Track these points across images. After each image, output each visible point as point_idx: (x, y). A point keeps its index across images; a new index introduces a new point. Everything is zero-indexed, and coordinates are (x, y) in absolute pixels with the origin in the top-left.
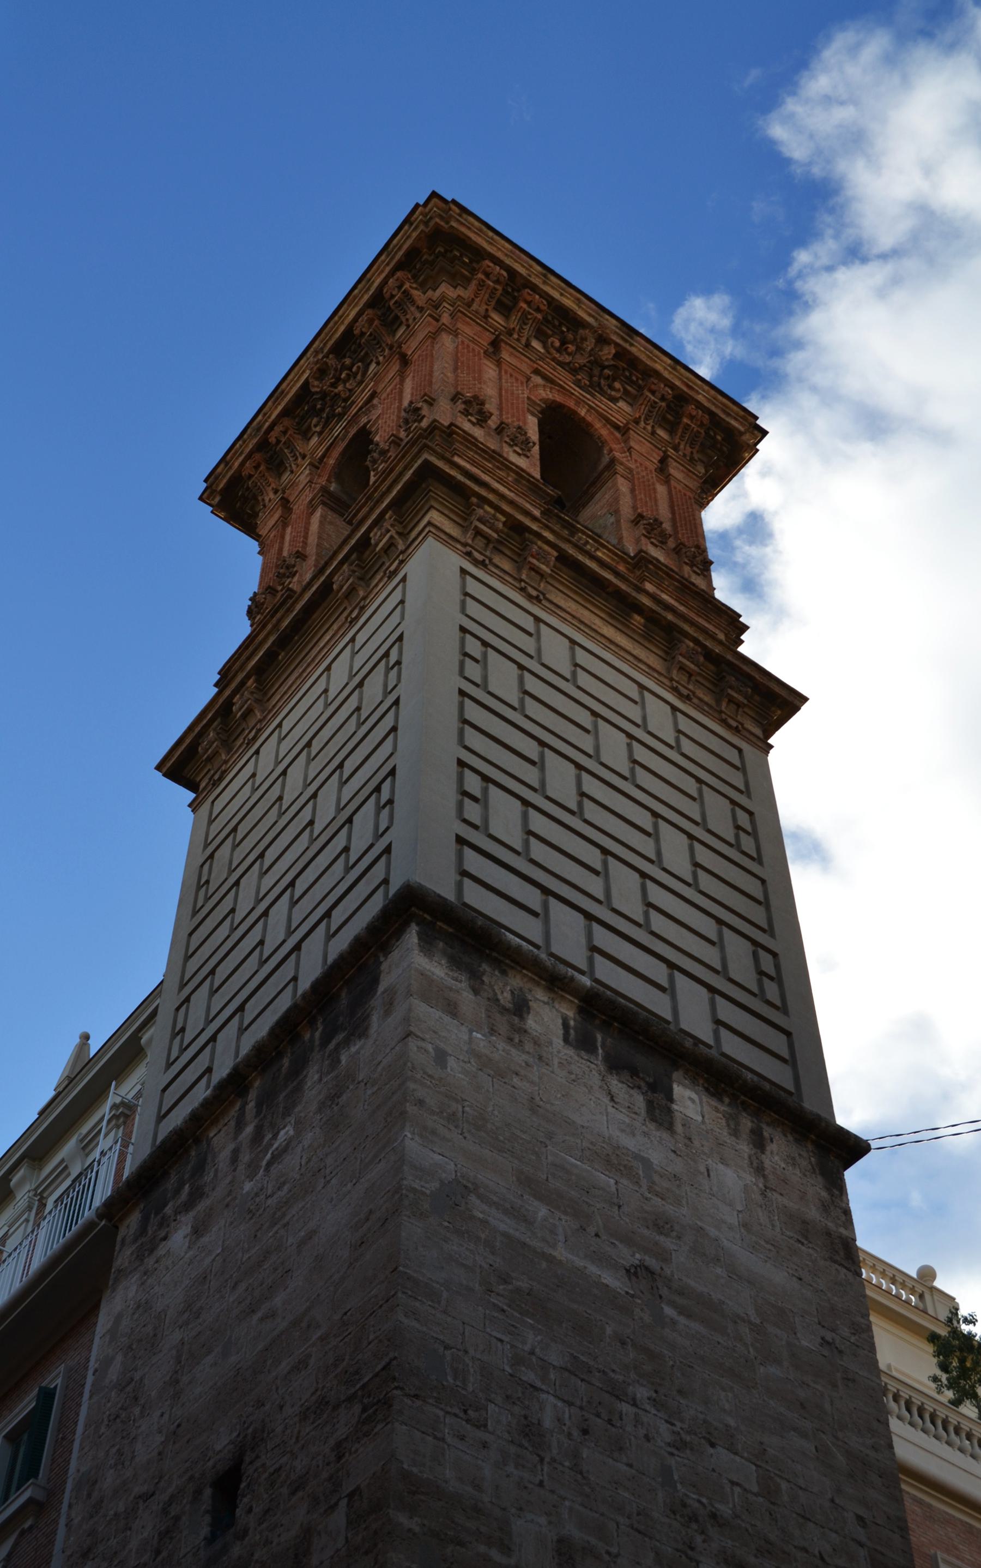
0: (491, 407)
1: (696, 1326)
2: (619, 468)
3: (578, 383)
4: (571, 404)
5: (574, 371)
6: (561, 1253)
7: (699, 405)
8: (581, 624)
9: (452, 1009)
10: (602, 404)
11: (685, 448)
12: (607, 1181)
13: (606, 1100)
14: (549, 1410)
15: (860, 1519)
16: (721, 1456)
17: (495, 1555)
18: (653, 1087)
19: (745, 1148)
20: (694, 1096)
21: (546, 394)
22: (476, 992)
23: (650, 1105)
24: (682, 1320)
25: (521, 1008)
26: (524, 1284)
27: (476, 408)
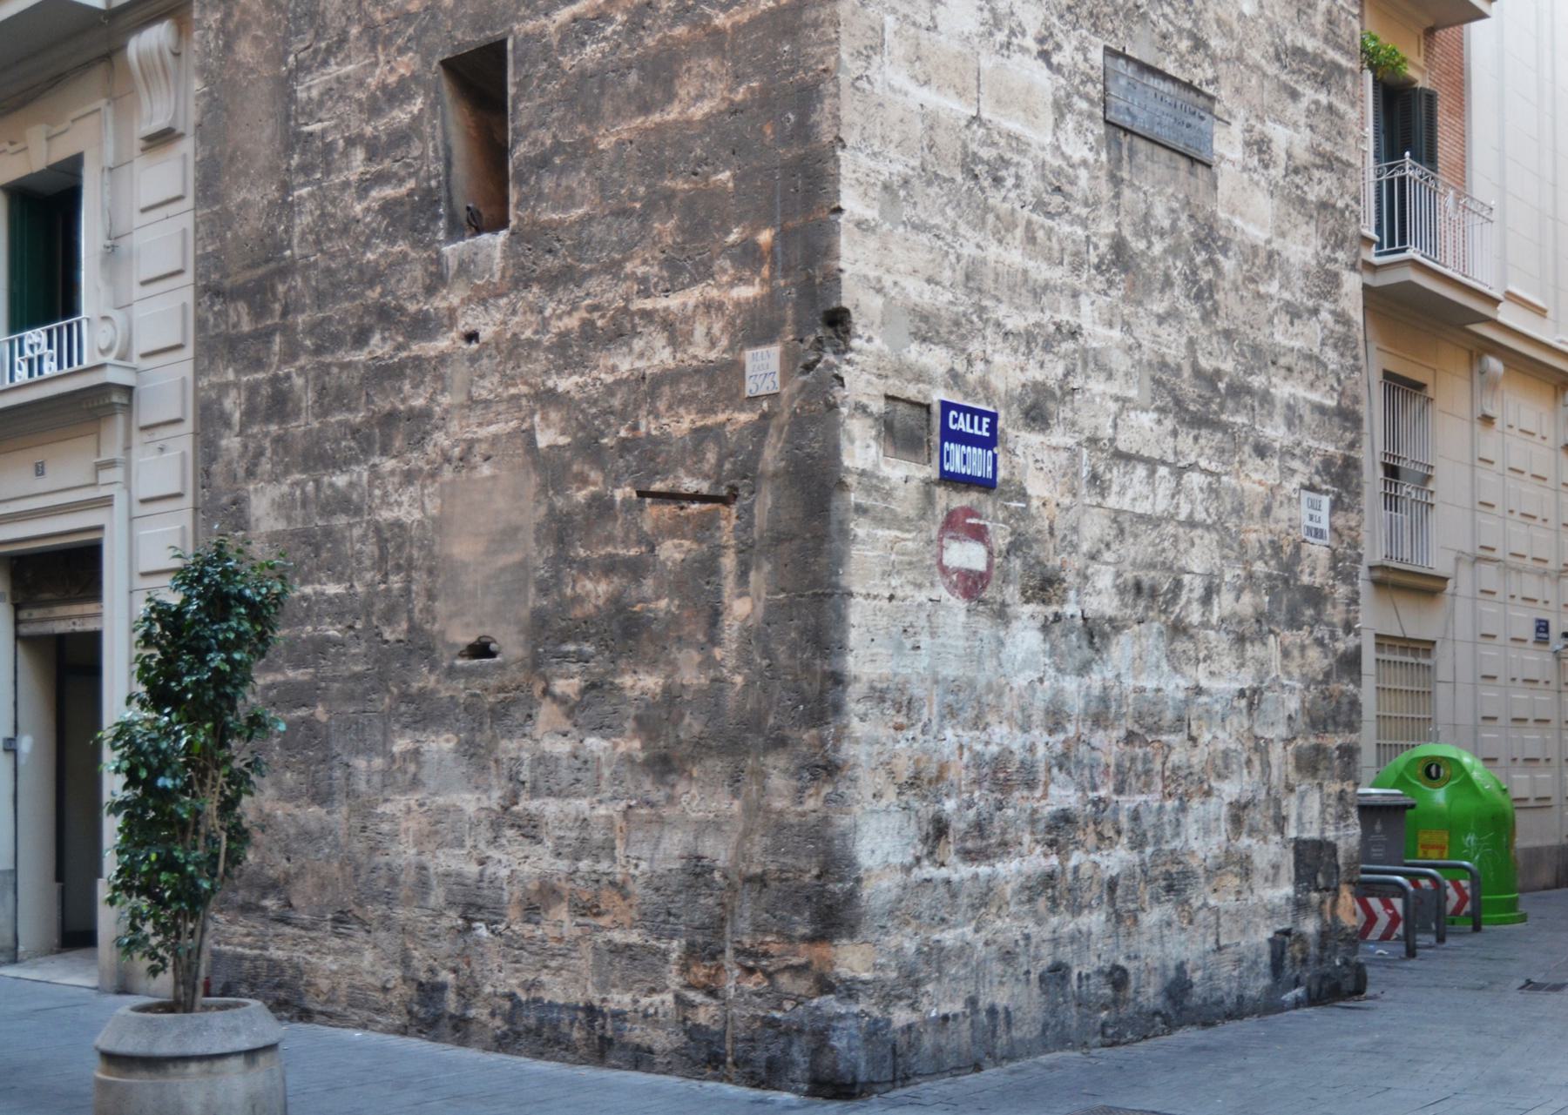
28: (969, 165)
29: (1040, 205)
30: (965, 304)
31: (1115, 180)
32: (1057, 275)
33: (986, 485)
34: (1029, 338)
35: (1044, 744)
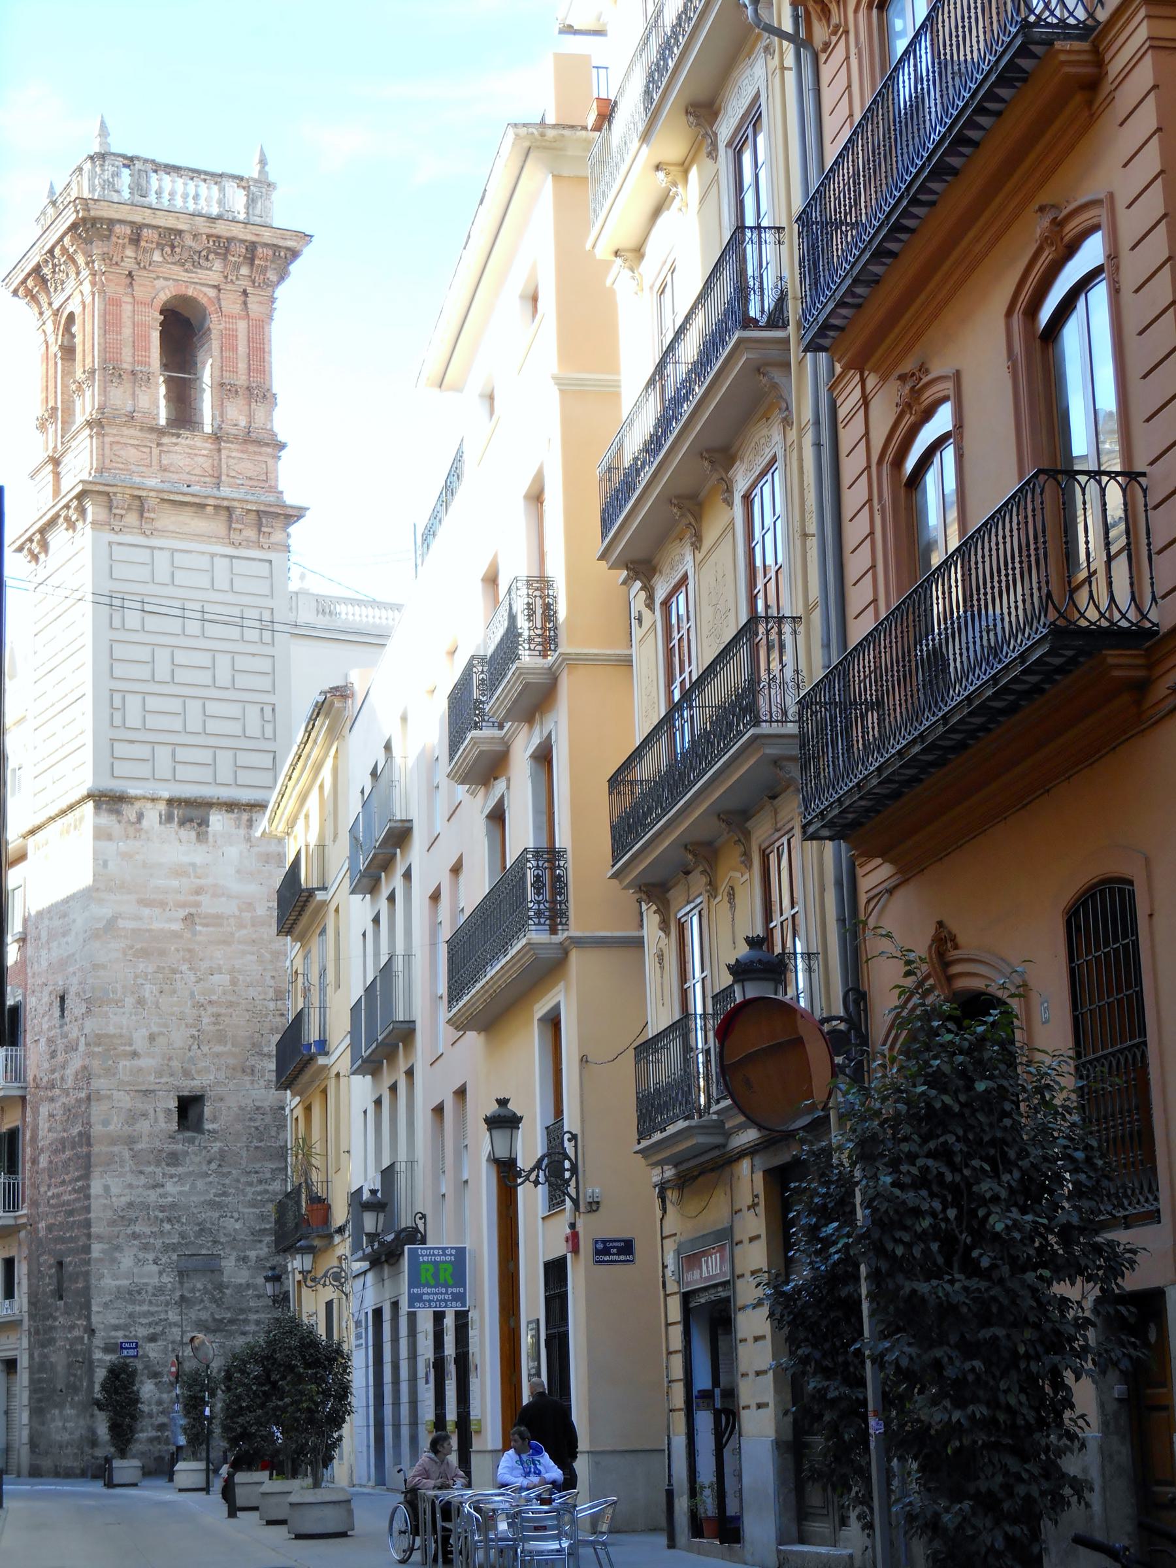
0: (127, 360)
1: (211, 929)
2: (214, 331)
3: (186, 271)
4: (182, 290)
5: (183, 265)
6: (156, 926)
7: (266, 245)
8: (177, 535)
9: (109, 837)
10: (203, 275)
11: (259, 279)
12: (175, 883)
13: (178, 843)
14: (149, 991)
15: (273, 977)
16: (216, 978)
17: (127, 1048)
18: (200, 825)
19: (242, 832)
20: (220, 817)
21: (165, 293)
22: (119, 822)
23: (198, 834)
24: (204, 929)
25: (140, 816)
26: (139, 946)
27: (117, 374)
28: (130, 1293)
29: (154, 1295)
30: (129, 1321)
31: (181, 1283)
32: (160, 1309)
33: (136, 1357)
34: (150, 1324)
35: (155, 1409)
